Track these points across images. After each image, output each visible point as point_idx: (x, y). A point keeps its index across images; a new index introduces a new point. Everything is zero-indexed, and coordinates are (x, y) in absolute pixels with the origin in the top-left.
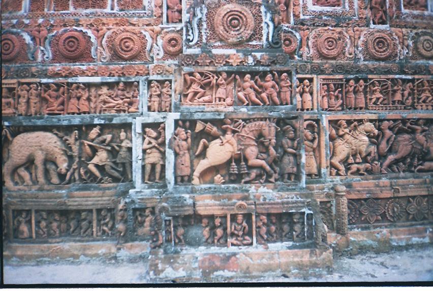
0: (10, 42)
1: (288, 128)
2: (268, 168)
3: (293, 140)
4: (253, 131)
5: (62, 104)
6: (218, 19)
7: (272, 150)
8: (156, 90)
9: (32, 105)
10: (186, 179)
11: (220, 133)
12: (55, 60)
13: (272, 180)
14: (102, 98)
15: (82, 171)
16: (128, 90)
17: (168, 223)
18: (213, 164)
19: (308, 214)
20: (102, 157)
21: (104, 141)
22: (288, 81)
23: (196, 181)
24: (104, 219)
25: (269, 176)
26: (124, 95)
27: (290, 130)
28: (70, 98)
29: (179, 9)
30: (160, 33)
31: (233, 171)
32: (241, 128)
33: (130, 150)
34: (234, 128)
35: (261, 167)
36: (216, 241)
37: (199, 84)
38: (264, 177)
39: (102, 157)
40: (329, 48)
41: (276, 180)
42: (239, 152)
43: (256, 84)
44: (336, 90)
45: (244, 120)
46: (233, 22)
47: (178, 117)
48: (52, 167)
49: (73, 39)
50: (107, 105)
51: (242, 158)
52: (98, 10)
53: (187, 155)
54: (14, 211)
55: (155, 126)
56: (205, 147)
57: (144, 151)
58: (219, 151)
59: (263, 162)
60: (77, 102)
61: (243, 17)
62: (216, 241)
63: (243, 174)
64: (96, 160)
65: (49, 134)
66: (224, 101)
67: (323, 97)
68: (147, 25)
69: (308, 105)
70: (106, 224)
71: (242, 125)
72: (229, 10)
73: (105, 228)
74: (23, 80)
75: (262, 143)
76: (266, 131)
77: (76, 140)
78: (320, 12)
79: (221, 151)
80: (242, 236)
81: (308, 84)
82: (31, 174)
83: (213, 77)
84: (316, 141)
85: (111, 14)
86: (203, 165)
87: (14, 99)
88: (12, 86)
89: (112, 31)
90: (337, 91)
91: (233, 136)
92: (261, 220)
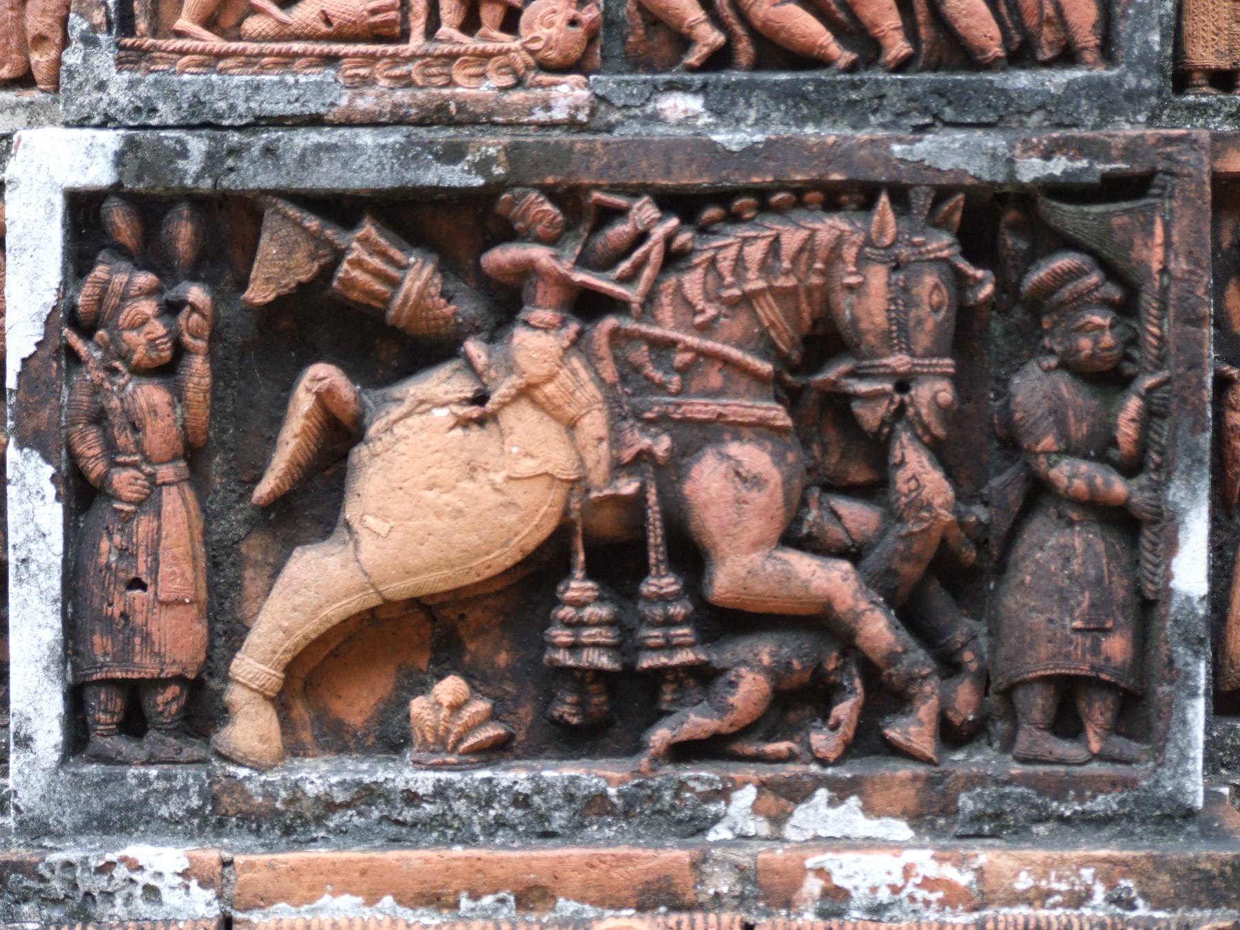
4: (748, 299)
7: (919, 472)
10: (167, 701)
11: (467, 307)
13: (914, 730)
18: (398, 588)
23: (250, 727)
25: (887, 696)
27: (1082, 301)
31: (574, 647)
32: (648, 273)
34: (580, 277)
35: (820, 622)
38: (845, 710)
41: (951, 735)
42: (628, 487)
47: (100, 174)
51: (655, 535)
53: (177, 507)
56: (339, 437)
58: (447, 480)
59: (831, 580)
63: (658, 674)
71: (653, 248)
75: (838, 405)
76: (870, 300)
79: (472, 470)
86: (310, 588)
91: (578, 343)
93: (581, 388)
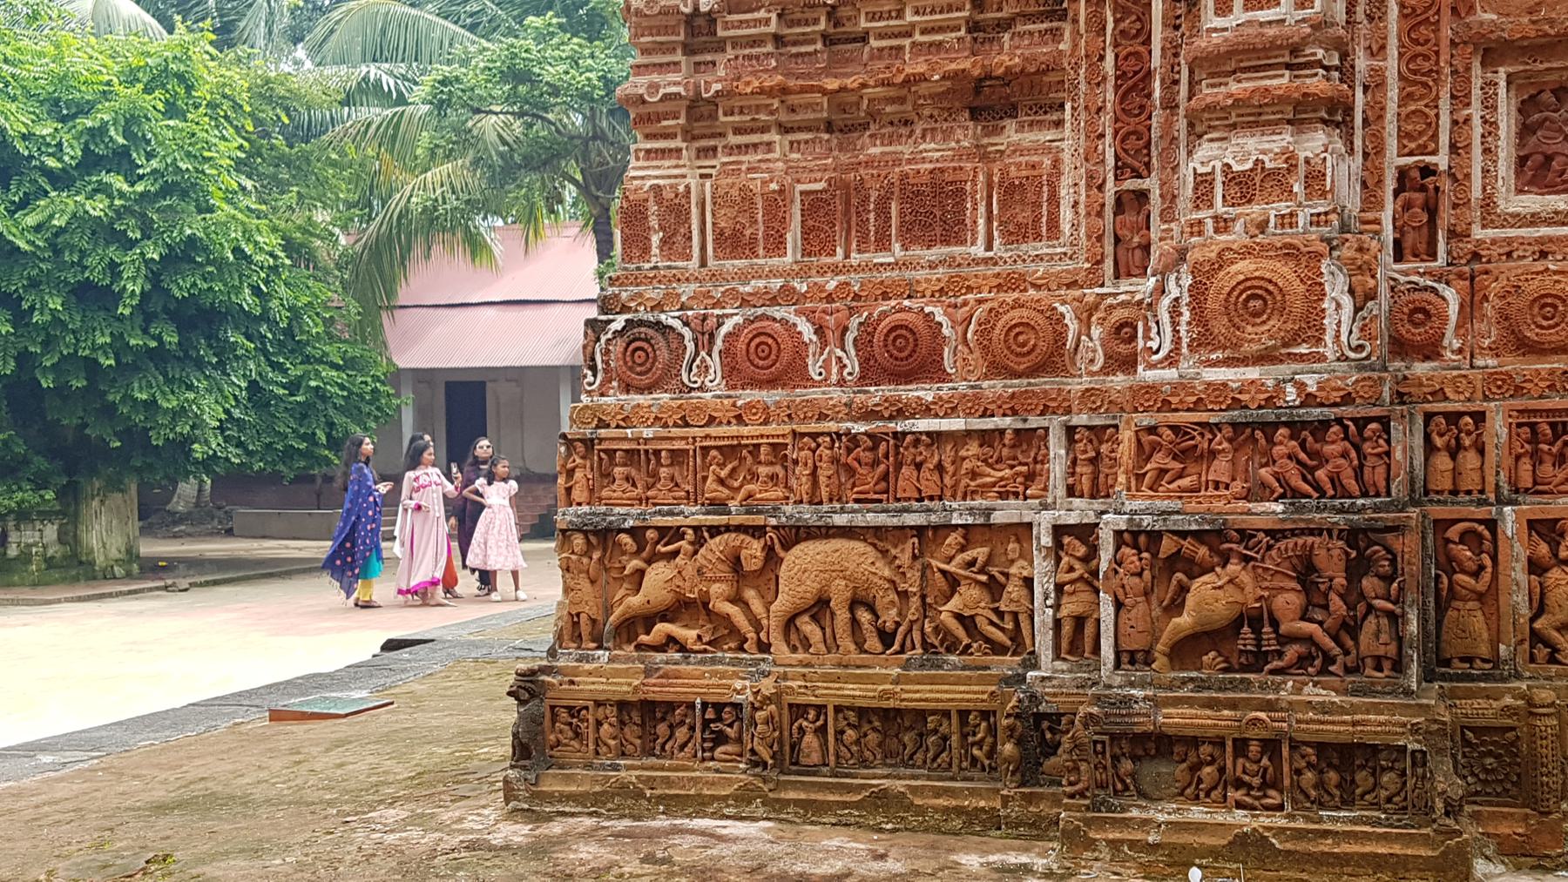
0: (770, 341)
1: (1375, 552)
2: (1328, 643)
3: (1388, 579)
5: (885, 477)
6: (1213, 304)
7: (1336, 603)
8: (1085, 451)
9: (822, 480)
10: (1139, 656)
12: (865, 378)
14: (967, 465)
15: (928, 628)
16: (1025, 447)
17: (1099, 747)
19: (1413, 752)
20: (968, 598)
21: (972, 563)
22: (1381, 441)
23: (1160, 662)
24: (974, 734)
25: (1329, 660)
26: (1015, 458)
28: (899, 466)
29: (1144, 242)
30: (1096, 307)
33: (1028, 582)
35: (1309, 639)
36: (1202, 795)
37: (1170, 452)
38: (1317, 662)
39: (968, 598)
40: (1545, 323)
43: (1304, 449)
44: (1556, 437)
45: (1267, 532)
46: (1252, 304)
48: (864, 616)
49: (904, 332)
50: (979, 481)
52: (957, 250)
54: (791, 706)
55: (1086, 532)
56: (1183, 590)
57: (1059, 588)
60: (915, 473)
61: (1276, 292)
62: (1202, 795)
64: (955, 604)
65: (859, 546)
66: (1227, 488)
67: (1518, 458)
68: (1069, 286)
69: (1470, 481)
70: (980, 744)
71: (1264, 544)
72: (1242, 277)
73: (976, 752)
74: (803, 429)
77: (915, 557)
78: (1533, 215)
80: (1259, 789)
81: (1471, 427)
82: (823, 629)
83: (1202, 435)
84: (1487, 576)
85: (986, 261)
87: (786, 468)
88: (781, 440)
89: (987, 306)
90: (1559, 443)
92: (1303, 757)
93: (1246, 578)
